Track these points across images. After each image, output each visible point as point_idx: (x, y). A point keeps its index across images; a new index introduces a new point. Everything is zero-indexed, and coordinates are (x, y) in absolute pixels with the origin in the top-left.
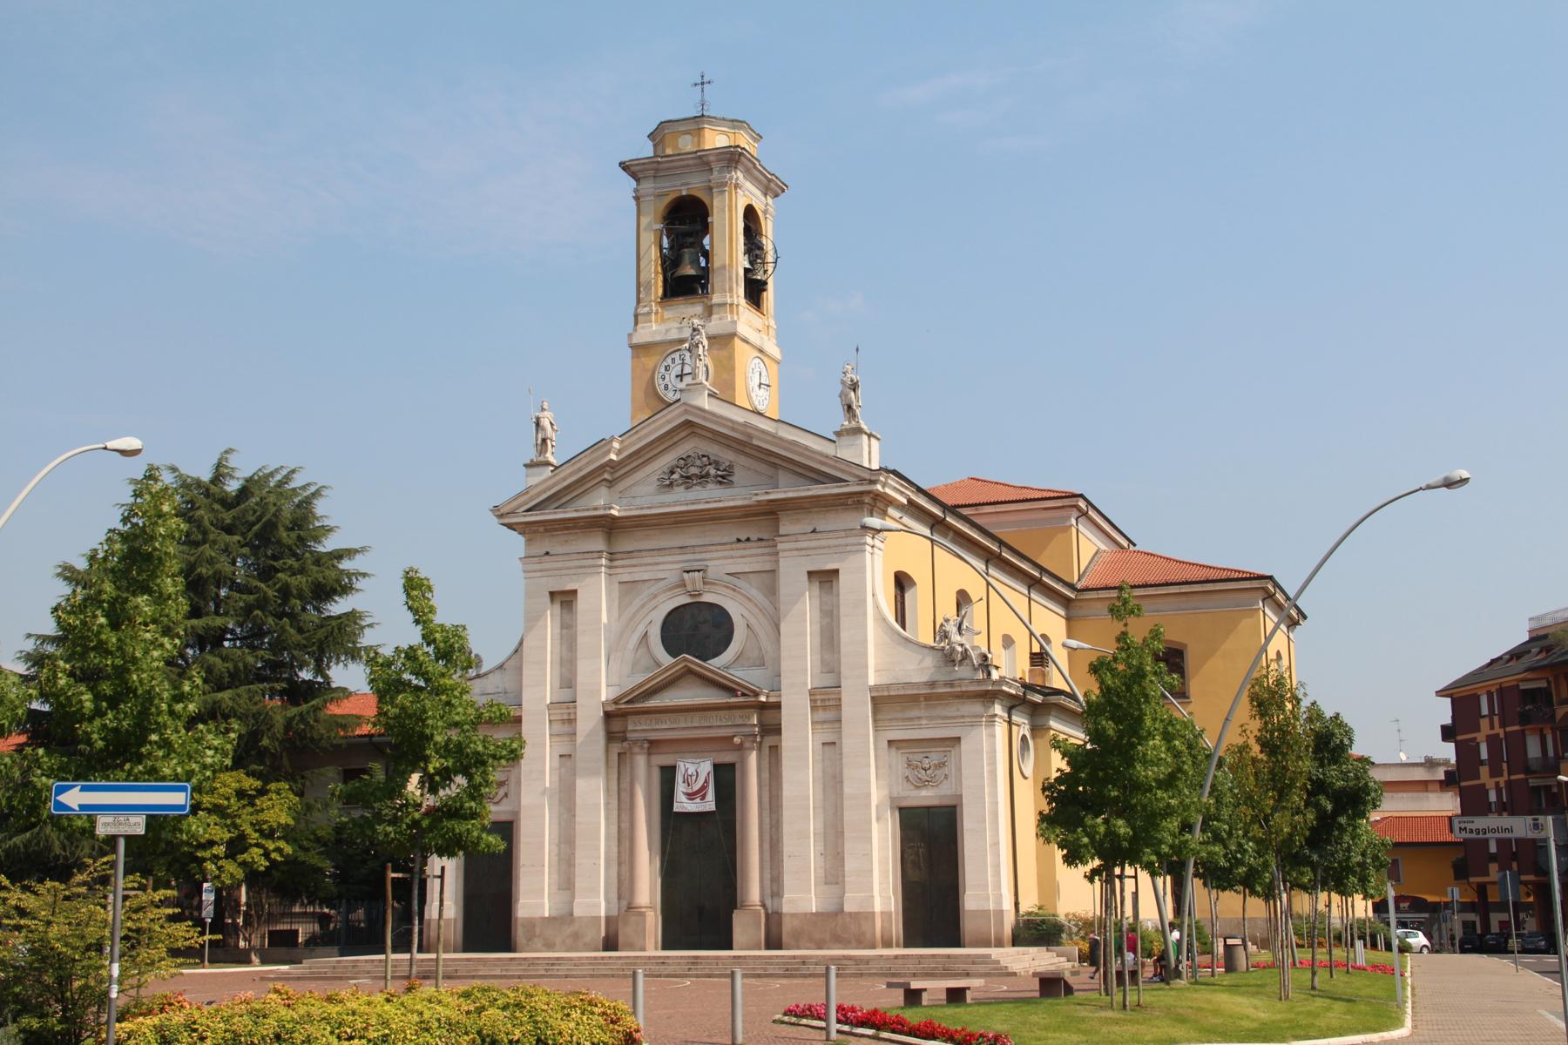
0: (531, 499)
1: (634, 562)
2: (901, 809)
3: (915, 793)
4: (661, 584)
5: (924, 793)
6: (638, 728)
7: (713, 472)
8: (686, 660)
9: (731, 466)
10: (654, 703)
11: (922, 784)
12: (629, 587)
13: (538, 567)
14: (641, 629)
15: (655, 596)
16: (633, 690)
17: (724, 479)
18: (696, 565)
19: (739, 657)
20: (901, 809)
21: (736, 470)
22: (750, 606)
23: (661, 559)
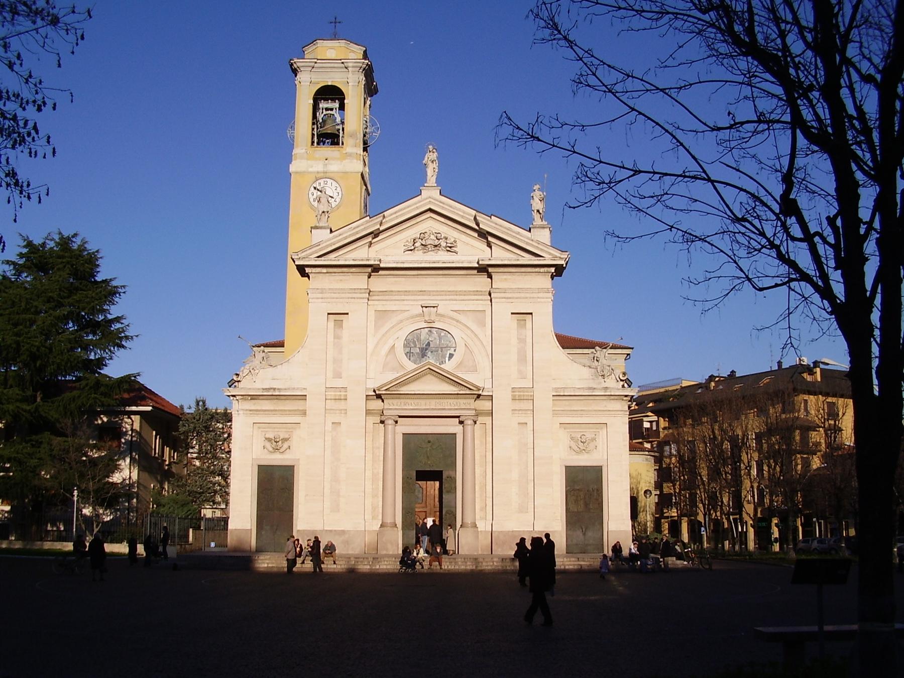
0: (320, 250)
1: (387, 297)
2: (566, 467)
3: (576, 457)
4: (406, 314)
5: (580, 457)
6: (393, 407)
7: (443, 244)
8: (429, 363)
9: (455, 242)
10: (404, 390)
11: (581, 451)
12: (382, 314)
13: (320, 296)
14: (390, 343)
15: (401, 321)
16: (391, 382)
17: (450, 249)
18: (432, 303)
19: (460, 365)
20: (566, 467)
21: (459, 244)
22: (469, 332)
23: (406, 298)
